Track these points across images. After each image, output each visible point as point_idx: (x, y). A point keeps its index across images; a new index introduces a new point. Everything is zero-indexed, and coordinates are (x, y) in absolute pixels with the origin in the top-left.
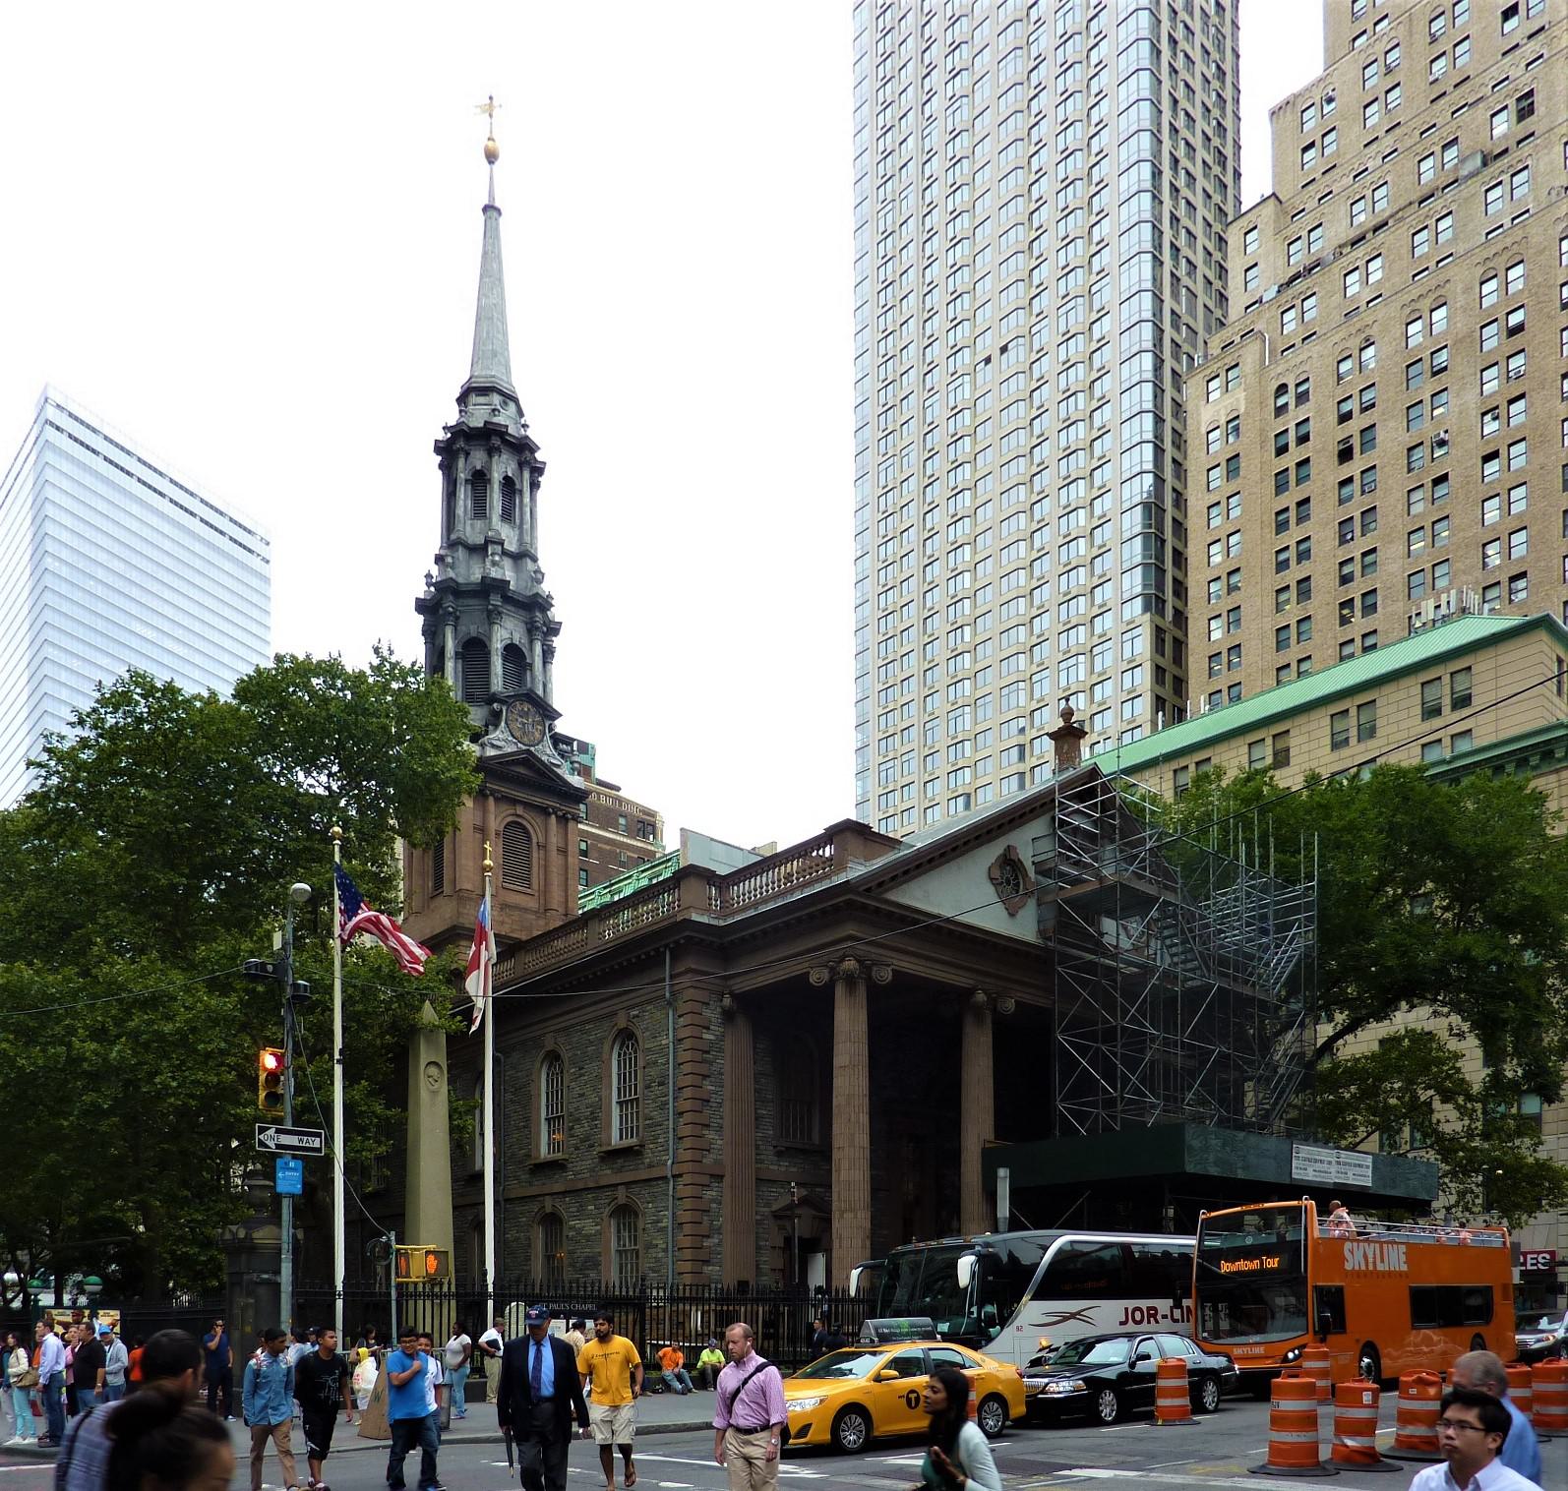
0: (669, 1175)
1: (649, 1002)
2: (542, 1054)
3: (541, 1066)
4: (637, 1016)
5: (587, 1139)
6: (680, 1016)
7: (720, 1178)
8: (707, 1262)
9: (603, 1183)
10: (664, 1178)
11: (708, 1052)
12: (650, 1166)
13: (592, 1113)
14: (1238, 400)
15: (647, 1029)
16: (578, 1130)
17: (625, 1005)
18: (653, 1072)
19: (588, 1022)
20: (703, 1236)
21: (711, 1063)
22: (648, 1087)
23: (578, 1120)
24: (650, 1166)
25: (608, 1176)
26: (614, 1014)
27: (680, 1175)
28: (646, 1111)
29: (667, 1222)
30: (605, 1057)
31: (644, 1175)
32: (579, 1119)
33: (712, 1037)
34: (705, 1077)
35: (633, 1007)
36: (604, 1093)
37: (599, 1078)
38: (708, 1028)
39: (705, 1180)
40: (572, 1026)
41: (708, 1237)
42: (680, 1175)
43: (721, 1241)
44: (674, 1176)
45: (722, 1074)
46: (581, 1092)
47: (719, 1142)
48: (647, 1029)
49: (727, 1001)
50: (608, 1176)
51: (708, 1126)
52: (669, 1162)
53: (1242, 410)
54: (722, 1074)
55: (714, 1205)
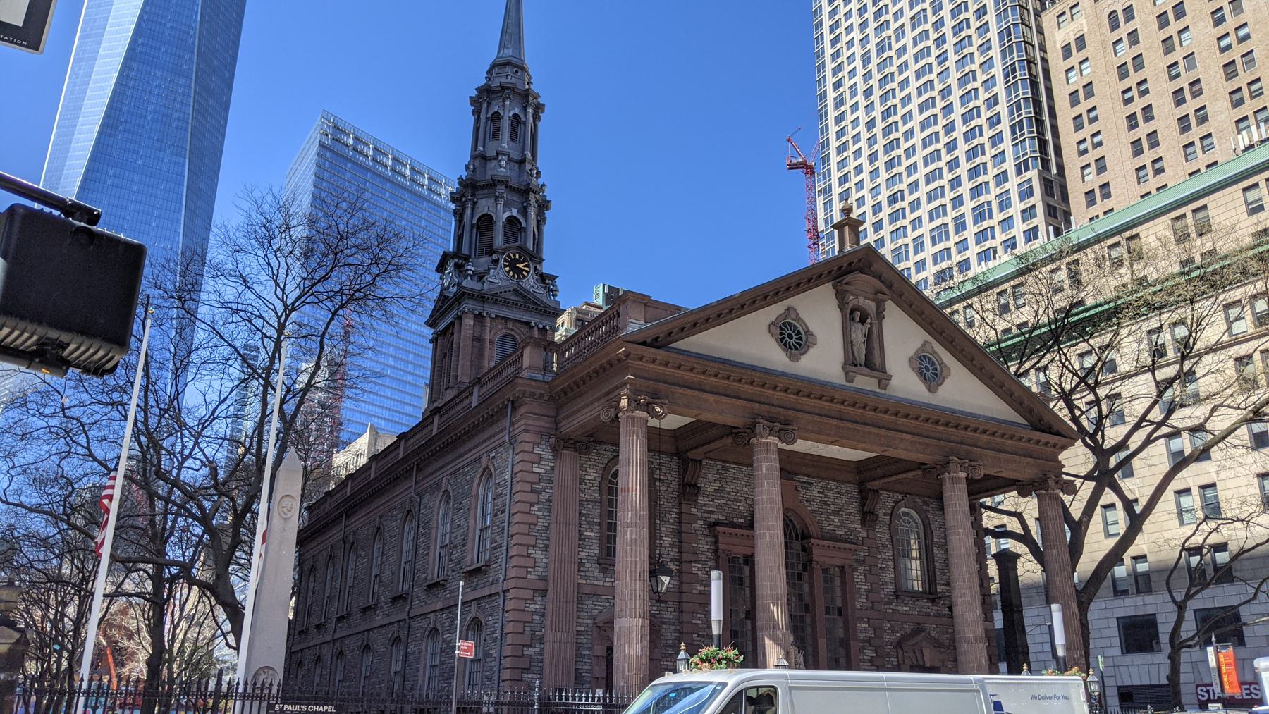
0: (500, 590)
1: (501, 445)
4: (494, 457)
5: (459, 562)
7: (544, 593)
8: (528, 670)
11: (539, 484)
14: (1081, 24)
17: (487, 449)
19: (468, 465)
20: (524, 646)
21: (538, 492)
23: (455, 546)
26: (480, 457)
29: (497, 635)
30: (474, 492)
32: (455, 546)
33: (543, 471)
34: (532, 504)
35: (488, 452)
36: (472, 522)
38: (539, 463)
39: (529, 594)
40: (458, 470)
41: (530, 646)
43: (542, 649)
44: (504, 592)
45: (551, 501)
47: (544, 560)
49: (553, 440)
51: (534, 546)
53: (1086, 30)
54: (551, 501)
55: (537, 617)
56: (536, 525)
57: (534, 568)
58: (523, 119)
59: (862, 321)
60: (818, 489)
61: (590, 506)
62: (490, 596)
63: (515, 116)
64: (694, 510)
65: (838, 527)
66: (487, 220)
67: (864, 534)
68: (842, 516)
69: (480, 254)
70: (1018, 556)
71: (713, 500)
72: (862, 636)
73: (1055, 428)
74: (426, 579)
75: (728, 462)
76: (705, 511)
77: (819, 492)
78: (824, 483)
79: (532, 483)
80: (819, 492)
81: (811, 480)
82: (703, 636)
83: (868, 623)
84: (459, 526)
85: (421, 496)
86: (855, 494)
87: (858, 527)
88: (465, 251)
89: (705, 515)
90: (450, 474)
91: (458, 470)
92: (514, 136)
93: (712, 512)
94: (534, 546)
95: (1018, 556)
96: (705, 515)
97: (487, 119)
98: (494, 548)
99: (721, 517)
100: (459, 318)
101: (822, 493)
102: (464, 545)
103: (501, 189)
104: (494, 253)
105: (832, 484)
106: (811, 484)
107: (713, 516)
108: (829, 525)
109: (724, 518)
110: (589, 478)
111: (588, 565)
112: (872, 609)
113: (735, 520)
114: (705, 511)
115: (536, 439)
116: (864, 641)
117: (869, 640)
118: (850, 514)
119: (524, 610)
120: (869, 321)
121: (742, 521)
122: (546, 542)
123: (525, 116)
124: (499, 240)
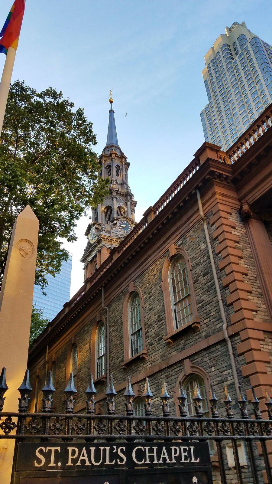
0: (226, 336)
2: (128, 295)
3: (128, 302)
4: (182, 244)
6: (212, 225)
9: (172, 362)
10: (224, 341)
11: (238, 243)
12: (207, 336)
13: (159, 317)
15: (189, 247)
16: (151, 332)
18: (198, 270)
22: (196, 281)
24: (207, 336)
25: (175, 356)
27: (237, 334)
28: (198, 298)
31: (203, 345)
32: (151, 325)
34: (240, 258)
37: (161, 293)
38: (234, 228)
39: (261, 335)
40: (143, 272)
42: (237, 334)
44: (231, 337)
46: (151, 307)
48: (189, 247)
50: (175, 356)
52: (225, 326)
57: (256, 311)
58: (121, 167)
62: (205, 349)
63: (118, 166)
66: (109, 209)
69: (107, 223)
74: (122, 361)
79: (236, 242)
84: (151, 309)
85: (109, 306)
88: (100, 221)
90: (135, 279)
91: (143, 272)
92: (118, 174)
97: (105, 168)
98: (201, 307)
100: (100, 251)
102: (161, 320)
103: (114, 194)
104: (114, 220)
115: (229, 210)
119: (260, 350)
122: (258, 290)
123: (122, 166)
124: (115, 215)
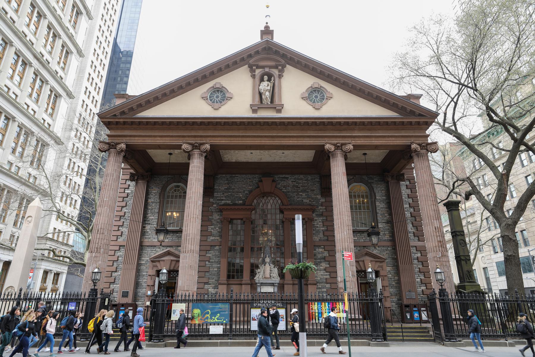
41: (116, 272)
56: (124, 216)
59: (269, 80)
60: (292, 180)
61: (154, 205)
64: (211, 200)
65: (305, 198)
67: (323, 200)
68: (308, 192)
70: (459, 202)
71: (223, 194)
72: (319, 256)
73: (417, 112)
75: (234, 174)
76: (218, 200)
77: (292, 182)
78: (296, 176)
80: (292, 182)
81: (287, 176)
82: (212, 262)
83: (324, 248)
86: (318, 180)
87: (319, 197)
89: (218, 202)
93: (223, 200)
94: (122, 226)
95: (459, 202)
96: (218, 202)
99: (227, 202)
101: (295, 182)
105: (302, 176)
106: (287, 178)
107: (223, 202)
108: (298, 198)
109: (230, 202)
110: (154, 192)
111: (149, 232)
112: (327, 240)
113: (237, 202)
114: (218, 200)
116: (320, 259)
117: (324, 258)
118: (314, 190)
120: (273, 79)
121: (241, 202)
